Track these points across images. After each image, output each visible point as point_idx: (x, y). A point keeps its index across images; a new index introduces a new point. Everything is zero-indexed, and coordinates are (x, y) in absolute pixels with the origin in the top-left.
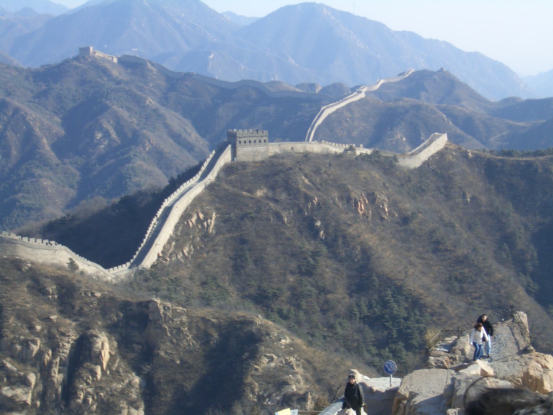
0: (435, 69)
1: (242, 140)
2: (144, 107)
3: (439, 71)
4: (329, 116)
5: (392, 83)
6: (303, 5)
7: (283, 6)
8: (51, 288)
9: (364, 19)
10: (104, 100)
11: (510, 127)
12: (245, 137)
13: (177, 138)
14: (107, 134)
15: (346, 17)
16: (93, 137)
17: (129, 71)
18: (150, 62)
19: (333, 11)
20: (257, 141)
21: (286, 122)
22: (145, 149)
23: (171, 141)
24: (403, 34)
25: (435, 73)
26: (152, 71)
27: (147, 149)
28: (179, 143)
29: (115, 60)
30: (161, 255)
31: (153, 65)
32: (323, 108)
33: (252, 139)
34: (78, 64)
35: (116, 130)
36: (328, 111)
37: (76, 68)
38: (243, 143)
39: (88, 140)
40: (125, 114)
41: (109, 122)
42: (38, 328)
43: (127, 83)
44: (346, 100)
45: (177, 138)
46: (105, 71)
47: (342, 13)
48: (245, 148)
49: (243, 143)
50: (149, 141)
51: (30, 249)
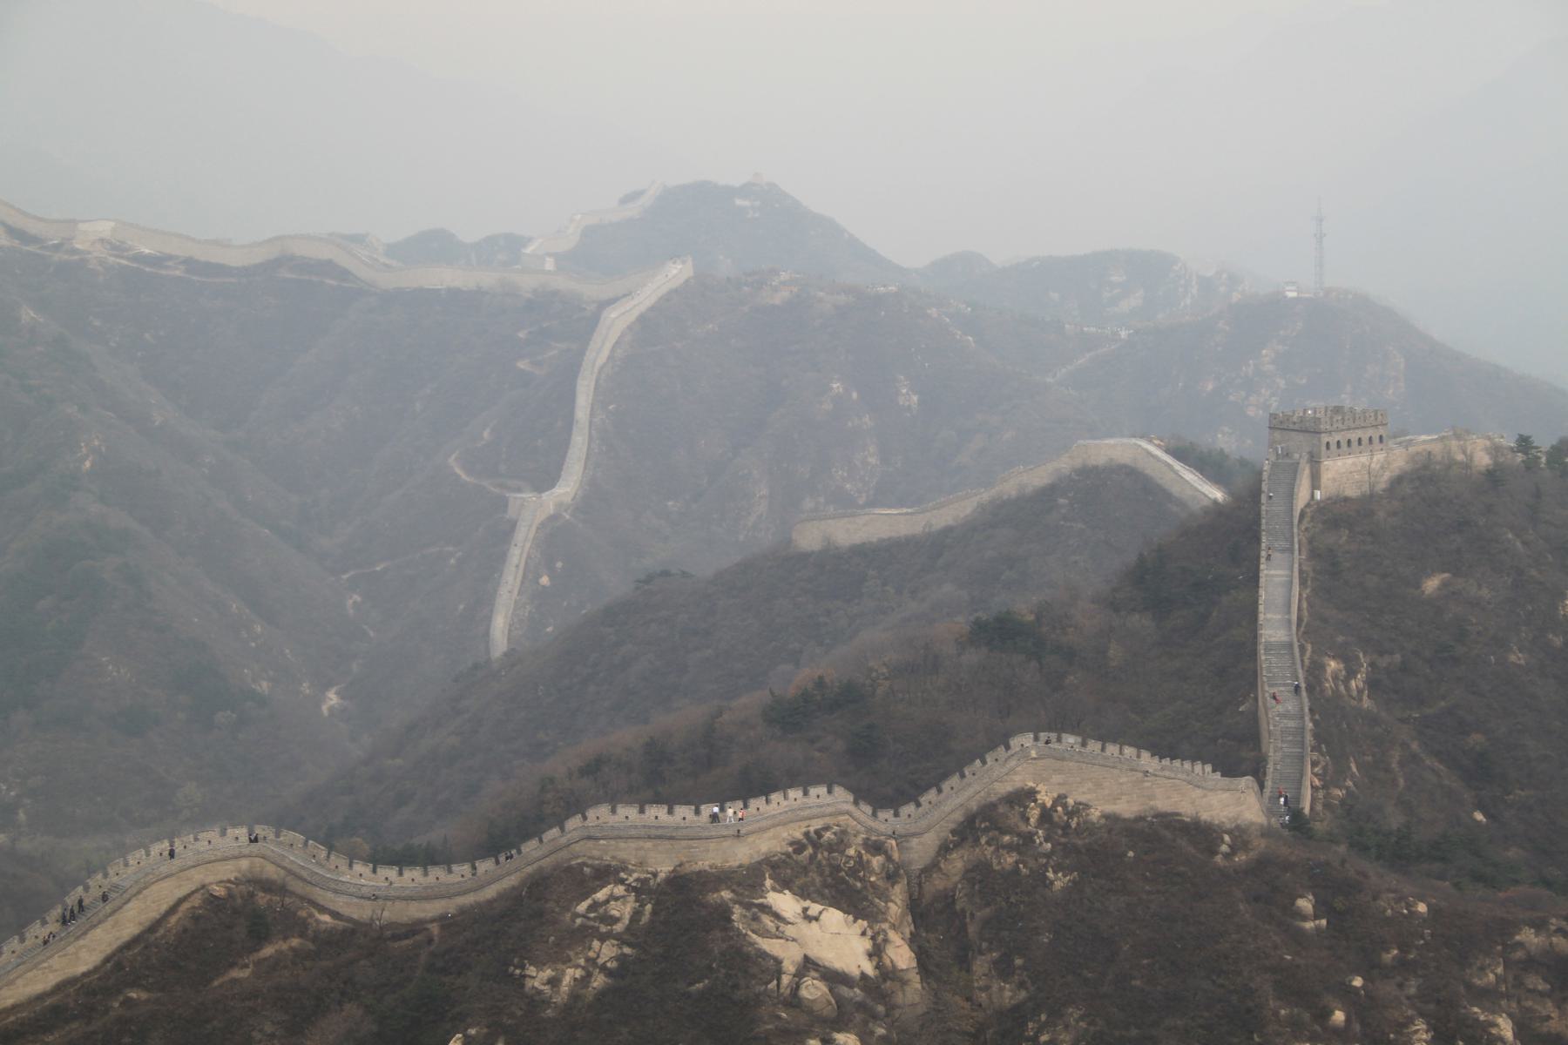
12: (1338, 430)
20: (1344, 444)
30: (1317, 782)
33: (1354, 436)
42: (1339, 1016)
48: (1339, 463)
49: (1333, 447)
51: (1199, 792)
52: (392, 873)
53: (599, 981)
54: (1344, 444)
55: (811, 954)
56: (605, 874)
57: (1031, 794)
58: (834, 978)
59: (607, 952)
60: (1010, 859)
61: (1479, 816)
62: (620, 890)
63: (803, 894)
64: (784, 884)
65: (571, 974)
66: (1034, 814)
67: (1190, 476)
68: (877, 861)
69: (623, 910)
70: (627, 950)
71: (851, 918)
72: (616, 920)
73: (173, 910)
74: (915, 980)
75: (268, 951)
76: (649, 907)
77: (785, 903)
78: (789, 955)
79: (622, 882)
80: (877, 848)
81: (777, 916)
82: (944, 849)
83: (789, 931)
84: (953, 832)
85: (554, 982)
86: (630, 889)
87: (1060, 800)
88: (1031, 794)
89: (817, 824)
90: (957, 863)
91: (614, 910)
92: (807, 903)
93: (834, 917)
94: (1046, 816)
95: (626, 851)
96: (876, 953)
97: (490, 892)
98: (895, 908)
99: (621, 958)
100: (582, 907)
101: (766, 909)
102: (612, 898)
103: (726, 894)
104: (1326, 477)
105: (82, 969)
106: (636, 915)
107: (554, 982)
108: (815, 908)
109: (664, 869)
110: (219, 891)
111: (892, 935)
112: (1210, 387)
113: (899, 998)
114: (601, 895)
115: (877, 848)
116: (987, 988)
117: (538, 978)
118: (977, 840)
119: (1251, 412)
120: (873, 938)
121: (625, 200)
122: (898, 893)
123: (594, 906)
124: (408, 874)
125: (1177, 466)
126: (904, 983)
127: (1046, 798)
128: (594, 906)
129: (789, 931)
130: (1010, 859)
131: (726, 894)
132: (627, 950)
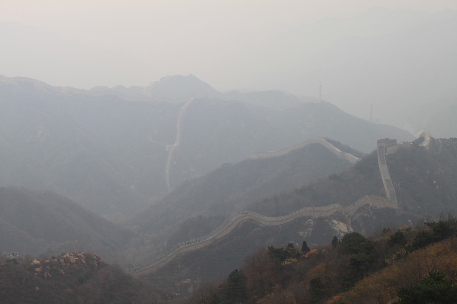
52: (271, 218)
53: (310, 234)
56: (309, 217)
57: (369, 205)
58: (344, 233)
59: (311, 229)
60: (366, 215)
61: (420, 207)
62: (311, 220)
63: (337, 220)
64: (334, 219)
65: (306, 233)
66: (369, 208)
67: (331, 145)
68: (347, 215)
69: (312, 223)
72: (311, 225)
73: (239, 224)
75: (254, 230)
77: (335, 222)
78: (337, 229)
80: (346, 213)
81: (335, 224)
85: (304, 234)
87: (373, 205)
88: (369, 205)
89: (337, 210)
91: (311, 223)
93: (342, 224)
94: (371, 208)
96: (348, 229)
97: (289, 221)
98: (350, 222)
100: (306, 223)
101: (333, 223)
102: (310, 221)
103: (327, 220)
105: (228, 233)
107: (304, 234)
108: (339, 222)
109: (317, 217)
110: (246, 221)
114: (309, 221)
115: (346, 213)
117: (301, 233)
122: (350, 220)
123: (308, 222)
124: (273, 218)
125: (329, 143)
127: (371, 205)
128: (308, 222)
130: (366, 215)
131: (327, 220)
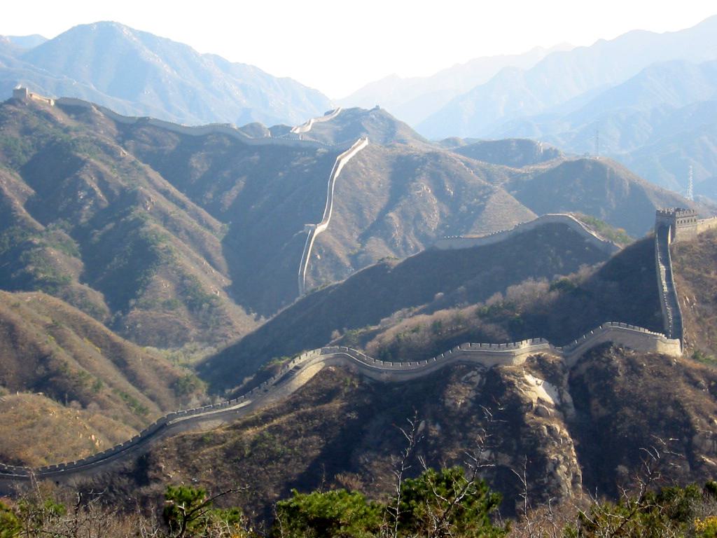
0: (368, 107)
1: (680, 220)
2: (120, 159)
3: (374, 109)
4: (345, 167)
5: (321, 123)
6: (99, 24)
7: (76, 25)
8: (703, 382)
9: (168, 40)
10: (73, 152)
11: (510, 174)
13: (166, 193)
14: (91, 193)
15: (146, 37)
16: (75, 197)
17: (73, 116)
18: (95, 105)
19: (131, 29)
20: (683, 222)
21: (280, 174)
22: (146, 208)
23: (162, 197)
24: (207, 55)
25: (371, 111)
26: (98, 115)
27: (149, 209)
28: (168, 198)
29: (53, 103)
31: (98, 108)
32: (338, 158)
33: (686, 219)
34: (16, 109)
35: (99, 186)
36: (344, 160)
37: (15, 113)
38: (680, 222)
39: (70, 200)
40: (104, 168)
41: (92, 178)
43: (76, 131)
44: (354, 148)
45: (166, 193)
46: (48, 117)
47: (141, 32)
49: (680, 222)
50: (149, 199)
54: (683, 222)
55: (540, 397)
57: (611, 343)
62: (476, 373)
70: (478, 394)
71: (551, 385)
74: (572, 405)
76: (485, 380)
79: (476, 370)
82: (579, 361)
83: (532, 388)
84: (584, 356)
86: (479, 373)
90: (583, 368)
92: (537, 379)
95: (478, 359)
99: (476, 396)
104: (677, 233)
106: (481, 382)
111: (564, 391)
112: (557, 191)
113: (567, 412)
114: (469, 375)
116: (597, 410)
118: (592, 359)
119: (572, 201)
120: (559, 392)
121: (327, 114)
126: (569, 407)
129: (532, 388)
132: (478, 394)
